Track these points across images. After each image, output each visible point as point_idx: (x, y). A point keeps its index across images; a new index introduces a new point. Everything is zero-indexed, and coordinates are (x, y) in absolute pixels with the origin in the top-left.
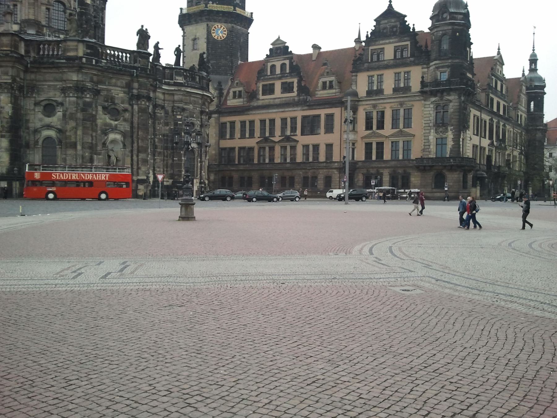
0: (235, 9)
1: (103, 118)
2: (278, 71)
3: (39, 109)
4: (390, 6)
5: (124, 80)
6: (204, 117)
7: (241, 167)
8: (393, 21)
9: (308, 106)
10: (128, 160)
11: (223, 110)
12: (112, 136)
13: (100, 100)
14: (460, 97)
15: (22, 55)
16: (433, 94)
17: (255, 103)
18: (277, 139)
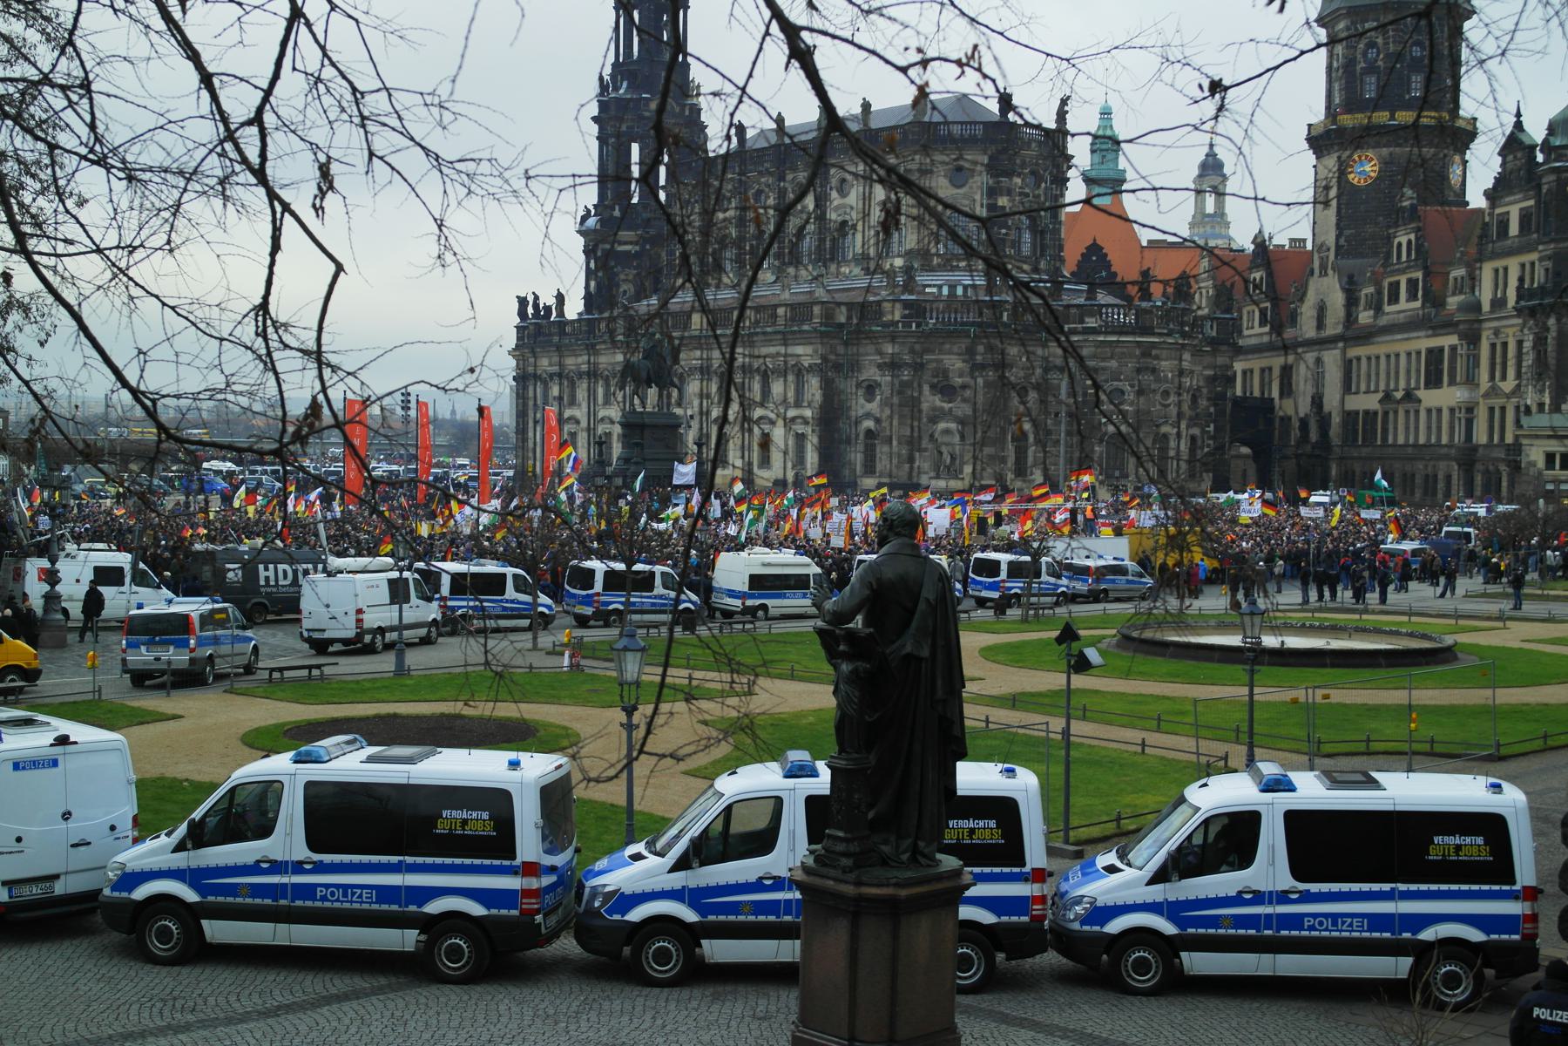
0: (1392, 117)
1: (931, 400)
2: (1404, 258)
3: (860, 392)
4: (1519, 125)
5: (963, 344)
6: (1147, 378)
7: (1365, 451)
8: (1519, 155)
9: (1432, 328)
10: (968, 456)
11: (1354, 335)
12: (942, 425)
13: (927, 376)
14: (1559, 320)
15: (841, 326)
16: (1532, 312)
17: (1383, 321)
18: (1399, 395)
